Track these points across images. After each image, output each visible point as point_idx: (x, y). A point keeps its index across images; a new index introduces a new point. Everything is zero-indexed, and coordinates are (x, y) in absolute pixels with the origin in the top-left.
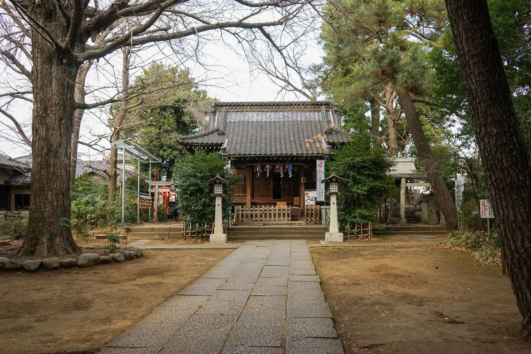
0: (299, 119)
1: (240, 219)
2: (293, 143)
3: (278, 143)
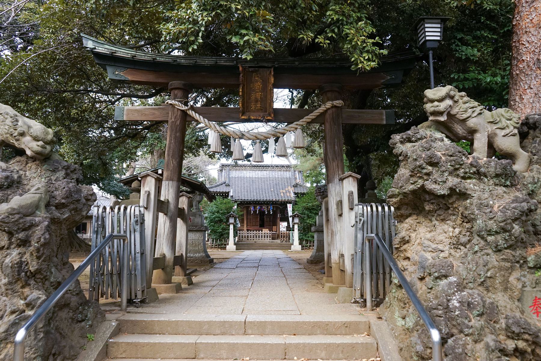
0: (277, 176)
1: (241, 239)
2: (273, 193)
3: (264, 193)
